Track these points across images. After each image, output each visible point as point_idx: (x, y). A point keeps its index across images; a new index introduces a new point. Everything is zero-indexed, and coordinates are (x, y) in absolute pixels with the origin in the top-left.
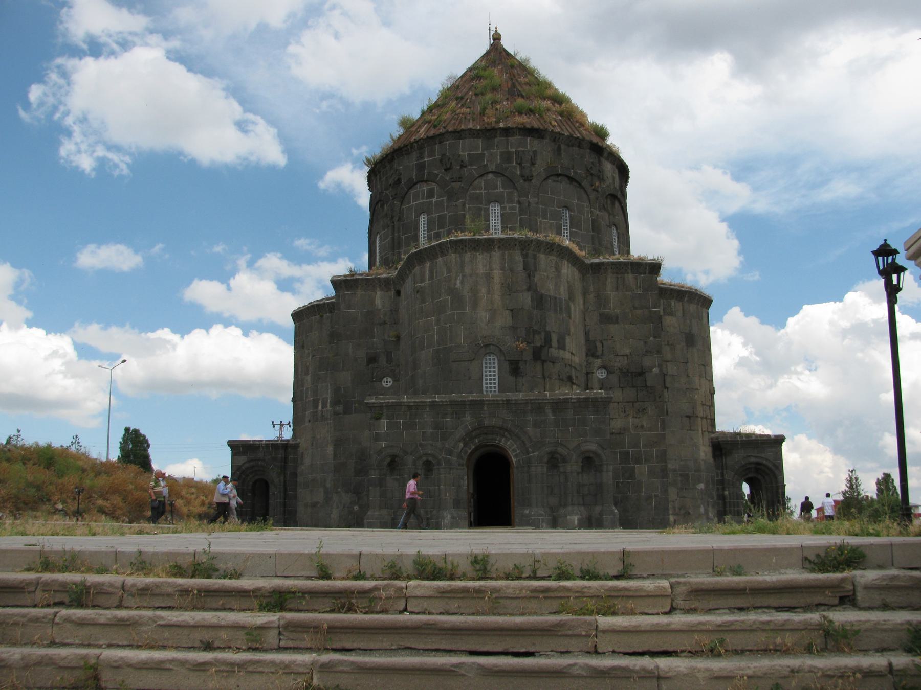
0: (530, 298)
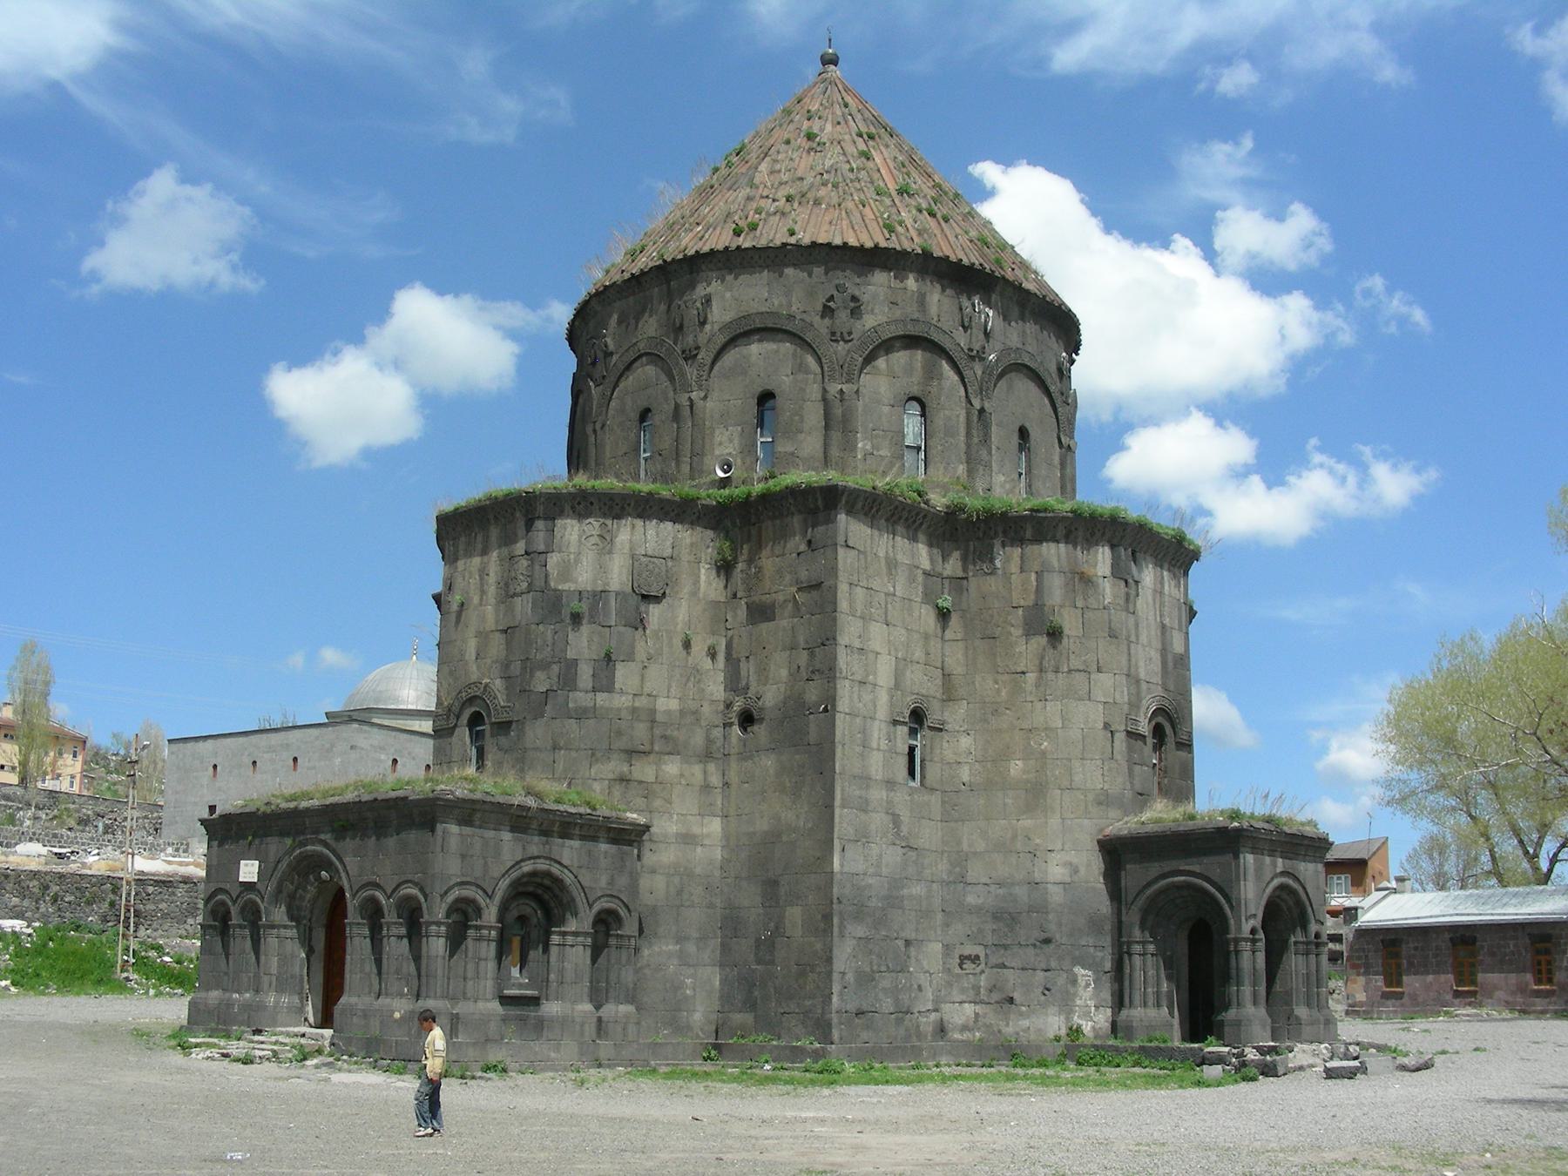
0: (530, 605)
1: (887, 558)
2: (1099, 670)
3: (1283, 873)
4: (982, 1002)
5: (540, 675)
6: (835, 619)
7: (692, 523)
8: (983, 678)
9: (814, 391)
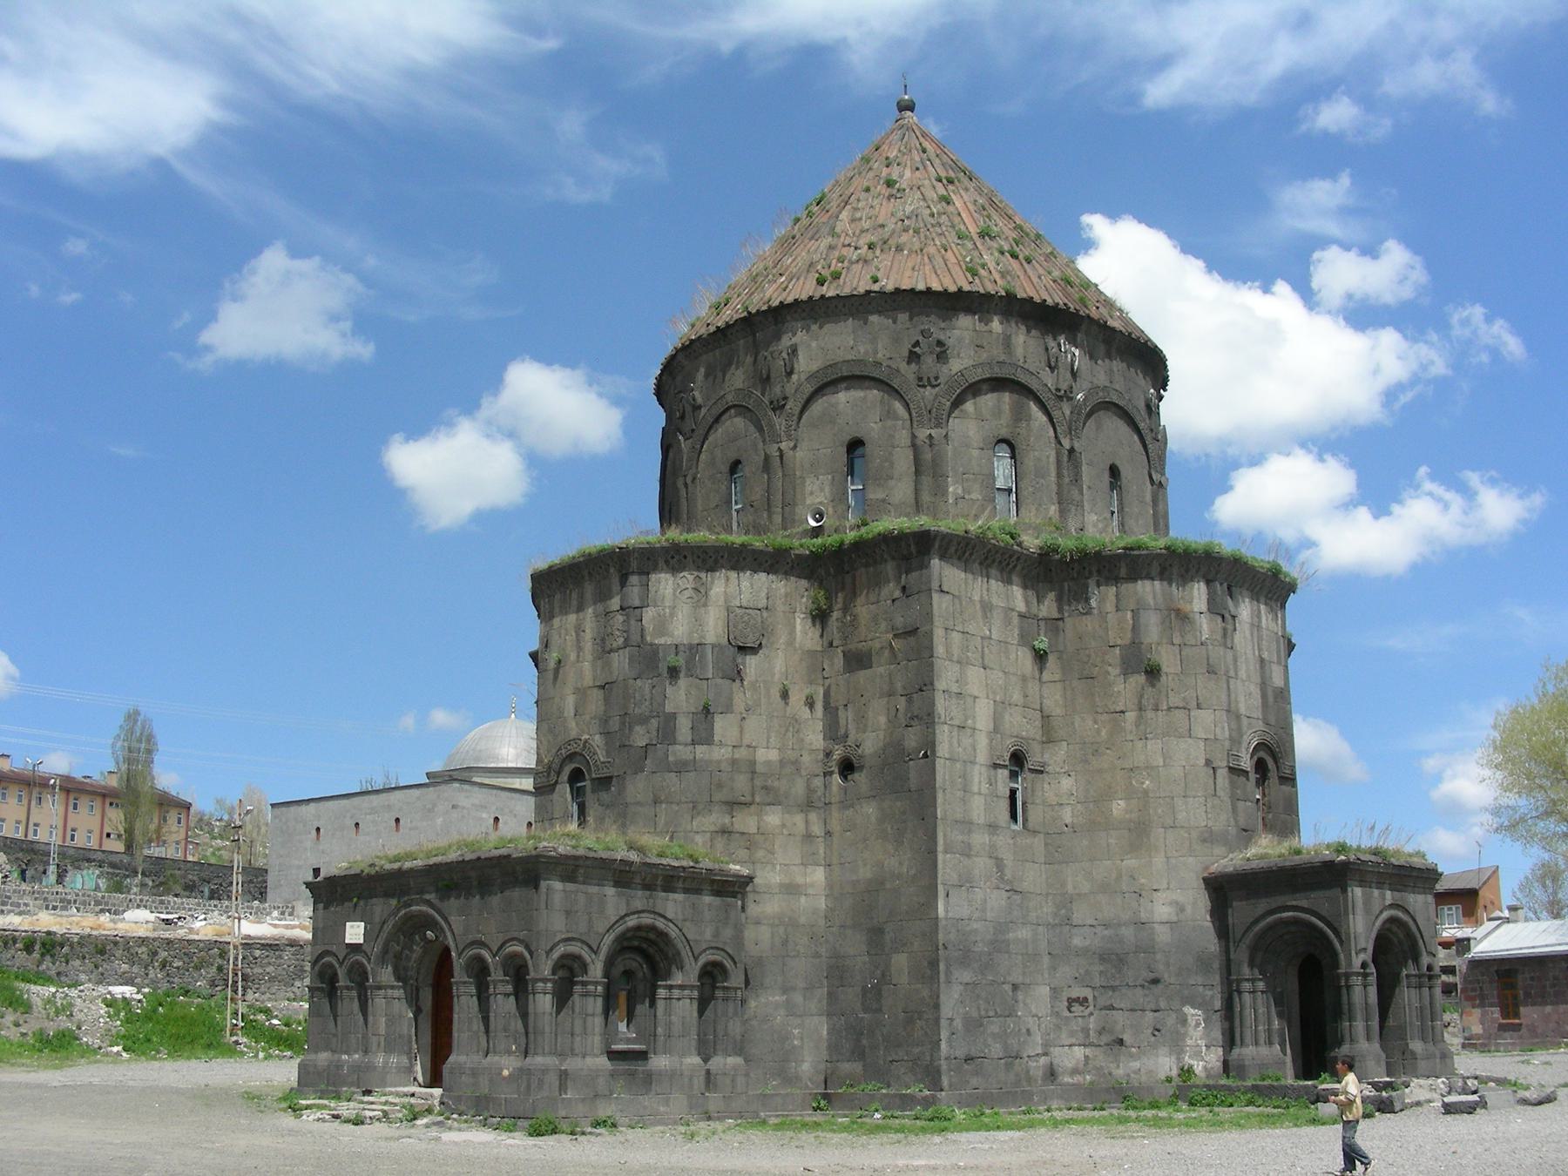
0: (627, 660)
1: (981, 601)
2: (1199, 707)
3: (1391, 906)
4: (1091, 1045)
5: (639, 729)
6: (931, 665)
7: (786, 573)
8: (1082, 718)
9: (903, 437)
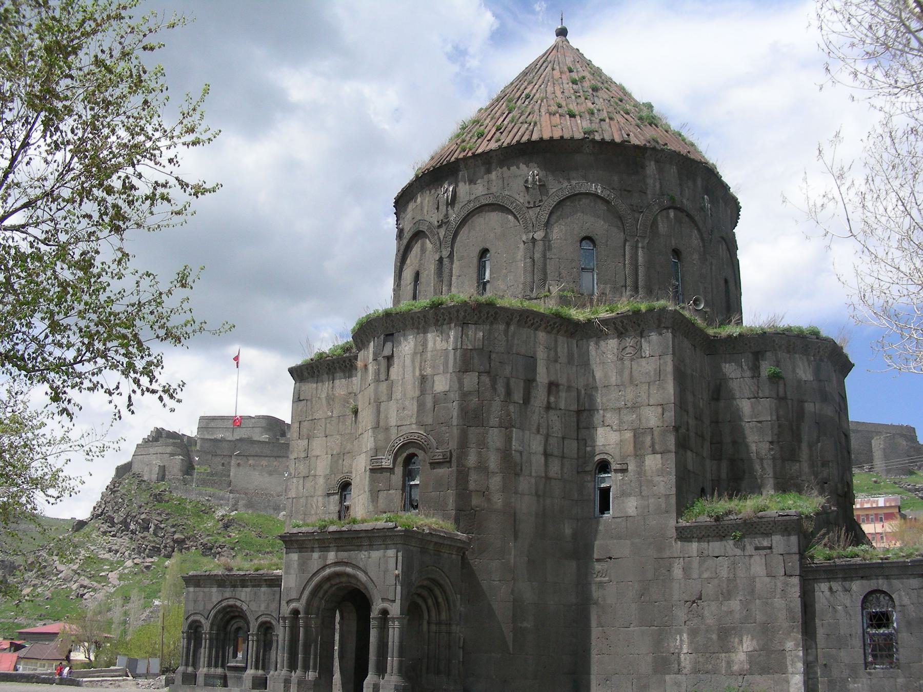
3: (336, 564)
